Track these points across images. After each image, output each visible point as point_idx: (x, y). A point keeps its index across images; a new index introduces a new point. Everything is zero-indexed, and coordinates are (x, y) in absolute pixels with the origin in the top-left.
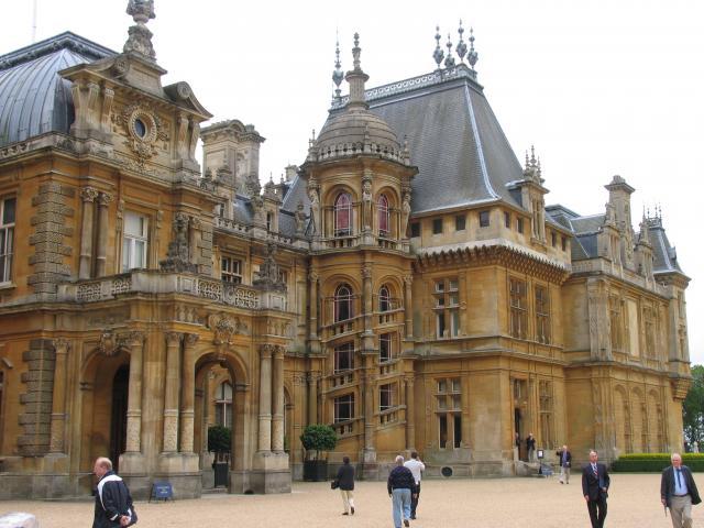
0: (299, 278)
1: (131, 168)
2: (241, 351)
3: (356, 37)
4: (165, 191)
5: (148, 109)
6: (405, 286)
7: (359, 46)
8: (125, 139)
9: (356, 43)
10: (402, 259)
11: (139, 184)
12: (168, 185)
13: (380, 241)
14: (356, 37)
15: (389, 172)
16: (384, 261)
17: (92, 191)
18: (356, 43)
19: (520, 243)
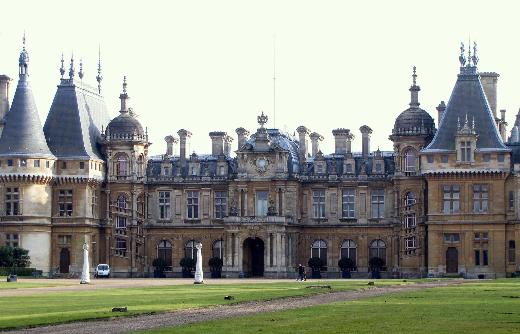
0: (390, 191)
1: (258, 177)
2: (262, 236)
3: (414, 68)
4: (271, 182)
5: (263, 156)
6: (421, 192)
7: (416, 74)
8: (256, 168)
9: (414, 72)
10: (417, 179)
11: (260, 182)
12: (270, 180)
13: (406, 173)
14: (414, 68)
15: (408, 140)
16: (406, 182)
17: (239, 189)
18: (414, 72)
19: (444, 168)
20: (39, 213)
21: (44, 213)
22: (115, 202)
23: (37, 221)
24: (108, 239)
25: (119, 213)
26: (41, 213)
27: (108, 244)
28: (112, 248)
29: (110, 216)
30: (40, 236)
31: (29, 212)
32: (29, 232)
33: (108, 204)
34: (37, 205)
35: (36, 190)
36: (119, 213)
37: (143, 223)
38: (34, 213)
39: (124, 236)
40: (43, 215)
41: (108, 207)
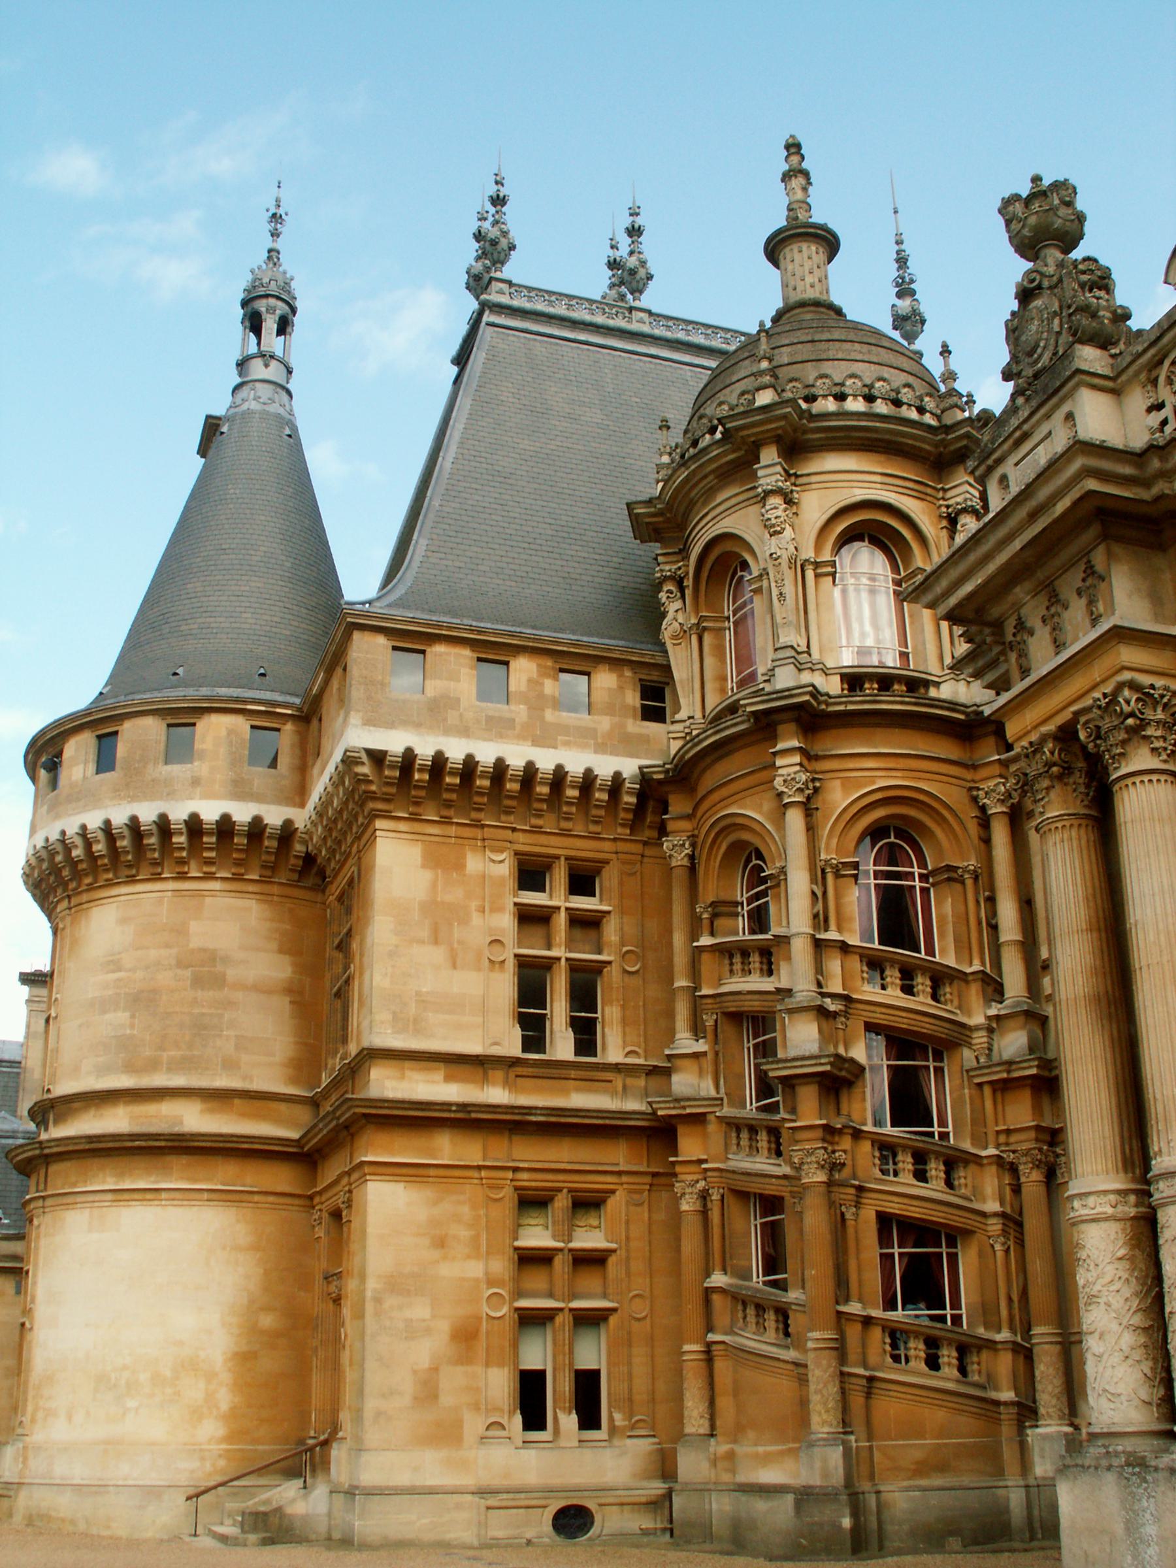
20: (130, 1068)
21: (175, 1066)
22: (722, 909)
23: (115, 1121)
24: (688, 1205)
25: (738, 984)
26: (153, 1065)
27: (690, 1244)
28: (718, 1279)
29: (697, 1030)
30: (137, 1219)
31: (76, 1070)
32: (68, 1199)
33: (679, 939)
34: (122, 1016)
35: (123, 921)
36: (738, 984)
37: (980, 1038)
38: (101, 1071)
39: (762, 1163)
40: (159, 1080)
41: (680, 960)
